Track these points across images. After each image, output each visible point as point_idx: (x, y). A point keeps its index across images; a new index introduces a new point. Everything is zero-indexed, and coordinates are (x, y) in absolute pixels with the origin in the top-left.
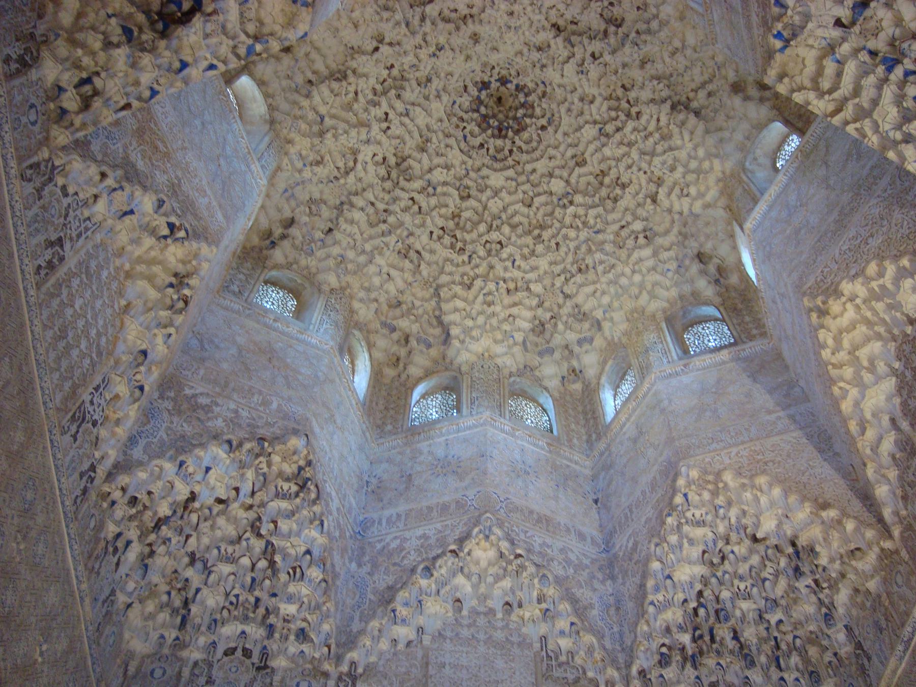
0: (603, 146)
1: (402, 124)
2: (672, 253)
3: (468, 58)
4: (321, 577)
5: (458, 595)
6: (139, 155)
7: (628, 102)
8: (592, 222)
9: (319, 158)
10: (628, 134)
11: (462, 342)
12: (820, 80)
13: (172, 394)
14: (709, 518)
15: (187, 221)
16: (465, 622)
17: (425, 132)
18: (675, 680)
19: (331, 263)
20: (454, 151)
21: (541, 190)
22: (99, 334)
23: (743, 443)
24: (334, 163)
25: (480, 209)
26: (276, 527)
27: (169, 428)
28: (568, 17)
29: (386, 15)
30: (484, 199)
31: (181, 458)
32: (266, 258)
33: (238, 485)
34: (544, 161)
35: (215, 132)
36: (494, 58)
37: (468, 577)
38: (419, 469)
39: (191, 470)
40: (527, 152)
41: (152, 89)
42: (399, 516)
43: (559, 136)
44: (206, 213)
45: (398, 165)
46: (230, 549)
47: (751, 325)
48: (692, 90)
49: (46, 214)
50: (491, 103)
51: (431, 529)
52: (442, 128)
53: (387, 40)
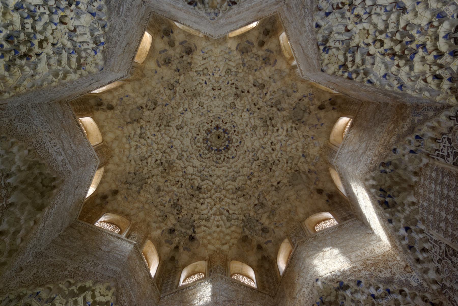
8: (170, 108)
14: (78, 45)
17: (254, 133)
19: (300, 90)
25: (224, 100)
26: (346, 27)
28: (195, 199)
29: (276, 206)
30: (223, 103)
43: (190, 135)
48: (134, 179)
52: (245, 134)
53: (274, 188)
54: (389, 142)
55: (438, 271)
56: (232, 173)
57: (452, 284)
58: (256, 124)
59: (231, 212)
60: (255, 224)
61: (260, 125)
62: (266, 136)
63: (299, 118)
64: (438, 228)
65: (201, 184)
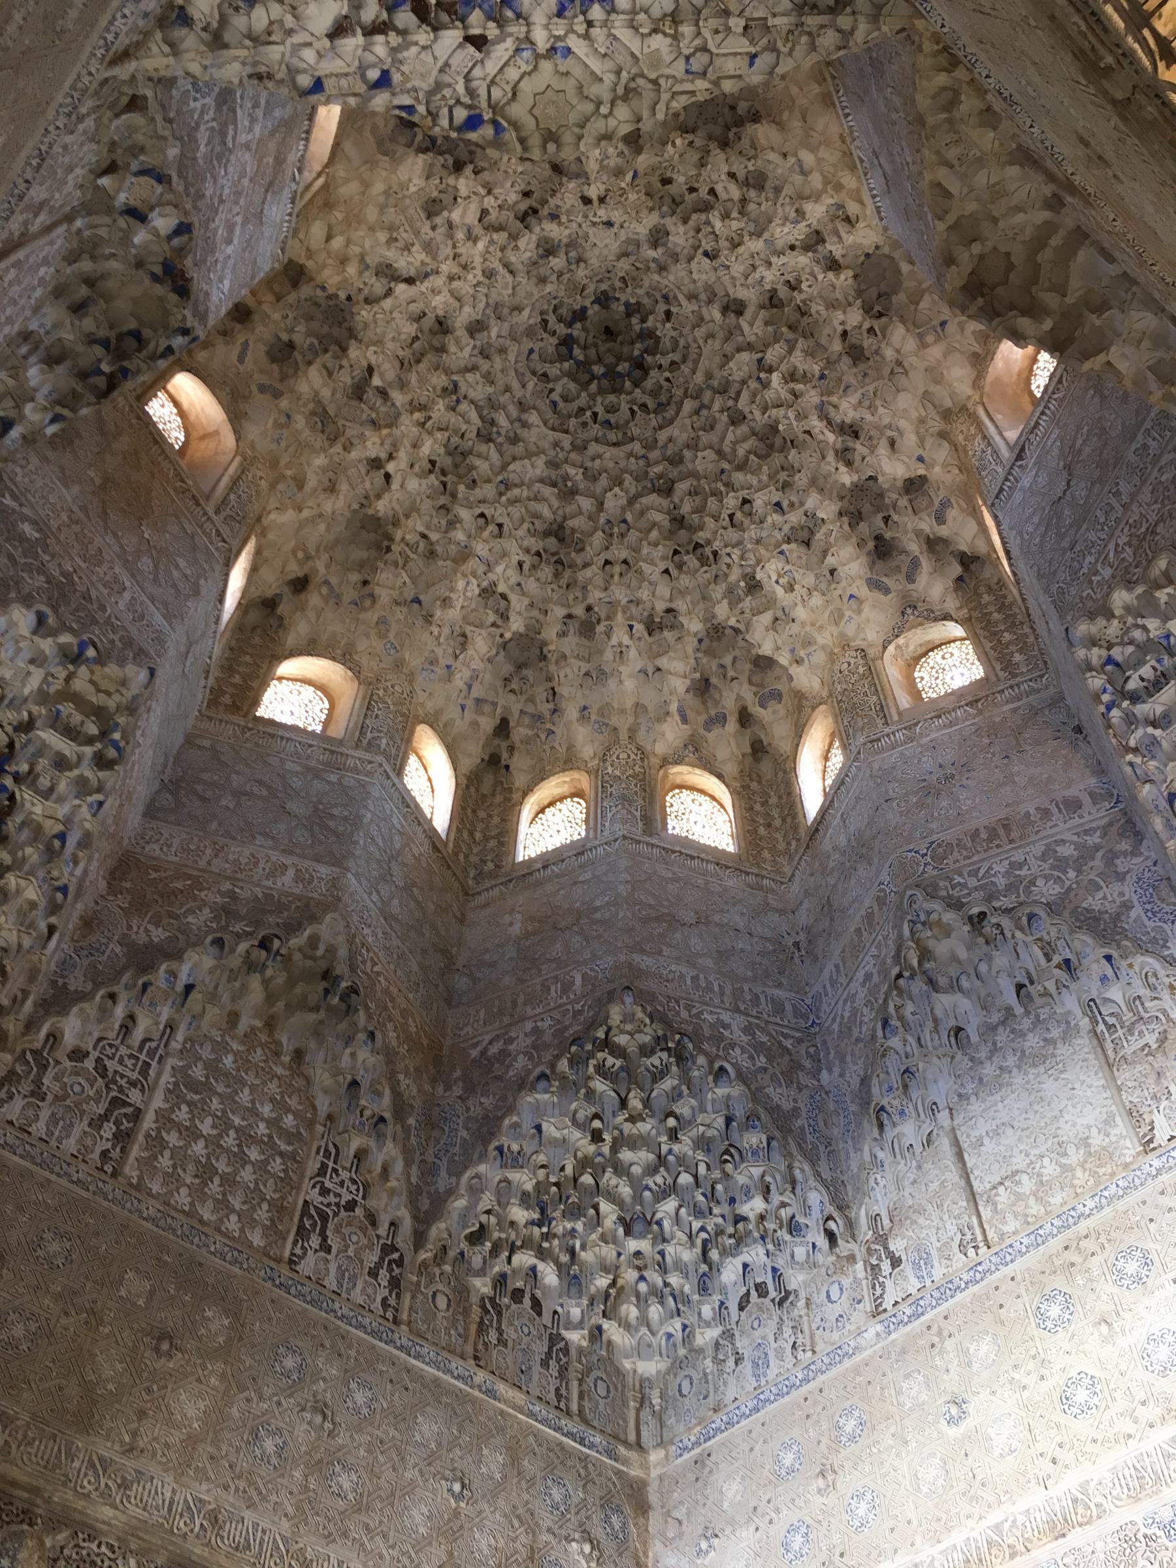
4: (764, 1138)
5: (952, 1023)
6: (151, 927)
7: (692, 190)
13: (458, 1073)
17: (553, 474)
20: (607, 455)
22: (273, 1123)
26: (677, 1118)
28: (513, 197)
29: (338, 448)
30: (690, 467)
32: (510, 790)
34: (706, 351)
35: (261, 783)
36: (526, 318)
37: (955, 986)
39: (515, 1147)
40: (684, 359)
42: (837, 966)
43: (688, 308)
44: (298, 890)
45: (561, 540)
46: (659, 1179)
49: (68, 1102)
50: (603, 348)
51: (869, 964)
53: (383, 456)
54: (390, 1019)
55: (78, 1055)
56: (494, 334)
57: (50, 1097)
58: (574, 507)
59: (401, 288)
60: (315, 325)
64: (173, 1093)
65: (537, 229)
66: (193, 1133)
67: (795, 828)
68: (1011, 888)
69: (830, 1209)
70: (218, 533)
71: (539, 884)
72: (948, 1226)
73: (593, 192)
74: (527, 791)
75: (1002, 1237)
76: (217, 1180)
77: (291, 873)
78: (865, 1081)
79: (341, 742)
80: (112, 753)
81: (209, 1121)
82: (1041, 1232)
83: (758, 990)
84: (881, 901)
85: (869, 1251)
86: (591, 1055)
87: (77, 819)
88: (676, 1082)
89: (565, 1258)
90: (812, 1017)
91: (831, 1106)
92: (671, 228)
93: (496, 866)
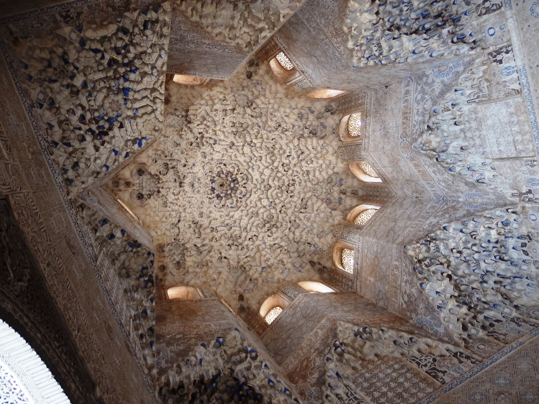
0: (220, 140)
1: (251, 229)
2: (253, 90)
3: (210, 212)
5: (459, 149)
6: (313, 376)
8: (256, 130)
9: (280, 262)
10: (211, 134)
11: (334, 168)
12: (149, 112)
13: (408, 314)
15: (331, 342)
16: (472, 143)
17: (249, 216)
18: (470, 27)
19: (322, 240)
21: (252, 155)
22: (395, 371)
23: (330, 41)
24: (279, 254)
26: (454, 249)
27: (425, 314)
28: (174, 184)
29: (210, 264)
30: (266, 177)
31: (436, 309)
32: (331, 269)
33: (440, 274)
34: (239, 159)
36: (206, 201)
37: (447, 145)
38: (401, 177)
39: (440, 302)
40: (238, 166)
41: (285, 391)
42: (428, 184)
44: (325, 330)
45: (268, 222)
47: (271, 45)
48: (178, 117)
50: (225, 188)
51: (430, 170)
52: (244, 209)
53: (219, 255)
56: (205, 211)
59: (180, 225)
60: (177, 253)
61: (261, 219)
62: (259, 229)
63: (289, 250)
64: (367, 394)
66: (384, 394)
67: (382, 188)
68: (423, 115)
69: (504, 209)
70: (212, 300)
71: (361, 268)
72: (524, 169)
73: (183, 162)
74: (334, 264)
75: (533, 151)
76: (404, 393)
77: (319, 331)
78: (467, 183)
79: (290, 304)
80: (254, 354)
81: (383, 388)
82: (536, 136)
83: (425, 211)
84: (412, 159)
85: (523, 200)
86: (421, 267)
87: (267, 374)
88: (442, 244)
89: (486, 306)
90: (441, 199)
91: (471, 200)
92: (204, 151)
93: (351, 281)
